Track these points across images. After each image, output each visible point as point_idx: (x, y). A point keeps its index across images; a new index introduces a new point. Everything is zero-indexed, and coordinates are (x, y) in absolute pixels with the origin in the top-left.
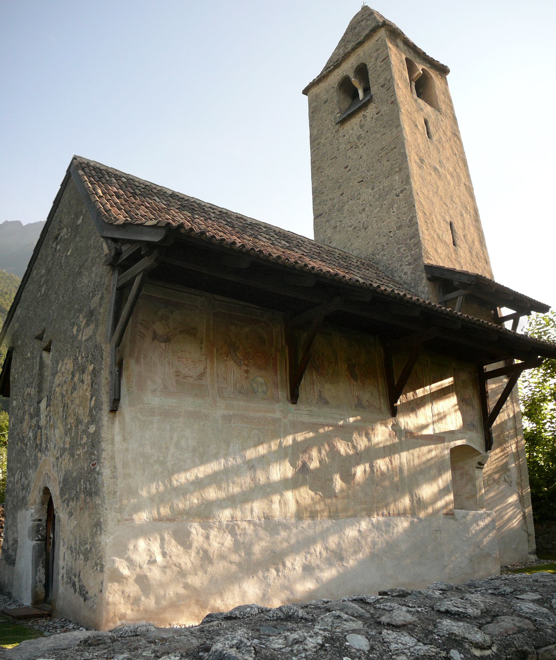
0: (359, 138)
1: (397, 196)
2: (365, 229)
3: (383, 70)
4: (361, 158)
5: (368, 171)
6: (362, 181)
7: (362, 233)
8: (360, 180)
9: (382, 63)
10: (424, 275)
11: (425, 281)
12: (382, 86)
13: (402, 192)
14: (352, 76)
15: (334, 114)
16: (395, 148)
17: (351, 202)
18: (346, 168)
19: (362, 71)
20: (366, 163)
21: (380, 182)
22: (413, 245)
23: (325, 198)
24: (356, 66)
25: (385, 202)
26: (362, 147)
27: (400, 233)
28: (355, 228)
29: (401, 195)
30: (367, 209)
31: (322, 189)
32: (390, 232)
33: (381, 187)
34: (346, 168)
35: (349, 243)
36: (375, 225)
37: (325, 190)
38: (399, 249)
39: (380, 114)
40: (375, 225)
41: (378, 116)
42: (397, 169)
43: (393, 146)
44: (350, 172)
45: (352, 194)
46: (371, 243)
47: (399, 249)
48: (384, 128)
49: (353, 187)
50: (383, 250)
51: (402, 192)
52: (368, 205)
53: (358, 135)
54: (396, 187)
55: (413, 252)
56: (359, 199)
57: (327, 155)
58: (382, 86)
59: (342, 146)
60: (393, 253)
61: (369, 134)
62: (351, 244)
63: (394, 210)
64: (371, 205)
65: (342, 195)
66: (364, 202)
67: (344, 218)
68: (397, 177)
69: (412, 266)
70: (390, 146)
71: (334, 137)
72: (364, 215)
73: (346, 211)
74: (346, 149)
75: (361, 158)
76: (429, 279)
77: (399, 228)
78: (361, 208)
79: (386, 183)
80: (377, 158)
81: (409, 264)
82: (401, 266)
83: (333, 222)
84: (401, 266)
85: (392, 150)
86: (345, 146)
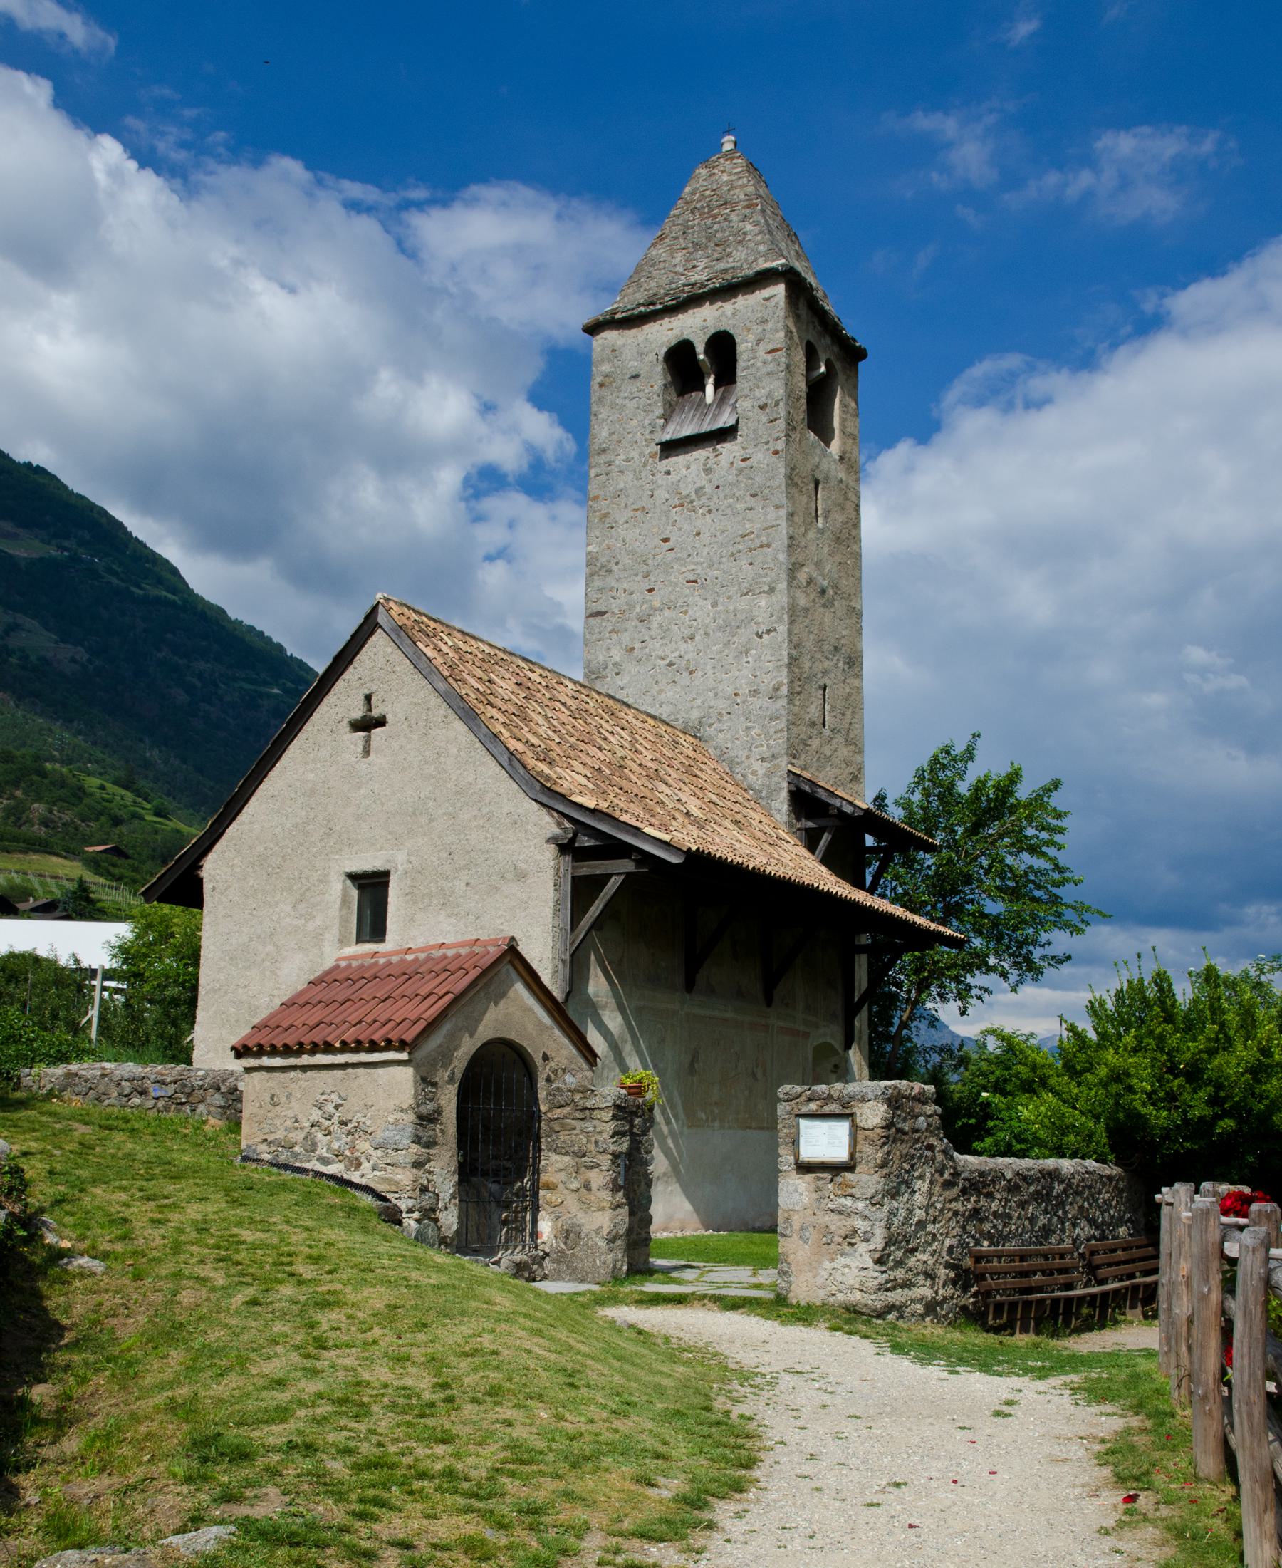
0: (699, 491)
1: (760, 636)
2: (691, 673)
3: (768, 374)
4: (698, 534)
5: (710, 566)
6: (695, 582)
7: (684, 679)
8: (692, 578)
9: (769, 357)
10: (785, 785)
11: (784, 795)
12: (762, 408)
13: (768, 631)
14: (700, 348)
15: (651, 416)
16: (768, 545)
17: (667, 613)
18: (666, 540)
19: (723, 345)
20: (706, 549)
21: (729, 598)
22: (773, 730)
23: (614, 584)
24: (712, 331)
25: (736, 639)
26: (703, 515)
27: (756, 703)
28: (671, 664)
29: (765, 636)
30: (697, 638)
31: (609, 562)
32: (736, 695)
33: (731, 608)
34: (666, 540)
35: (656, 688)
36: (710, 673)
37: (615, 568)
38: (748, 728)
39: (747, 463)
40: (710, 673)
41: (744, 464)
42: (766, 588)
43: (764, 540)
44: (671, 554)
45: (673, 597)
46: (699, 702)
47: (748, 728)
48: (753, 496)
49: (676, 585)
50: (720, 721)
51: (768, 631)
52: (701, 632)
53: (698, 485)
54: (760, 620)
55: (771, 742)
56: (686, 612)
57: (627, 496)
58: (762, 408)
59: (661, 494)
60: (737, 732)
61: (721, 492)
62: (660, 692)
63: (750, 659)
64: (707, 634)
65: (651, 590)
66: (695, 623)
67: (652, 638)
68: (763, 603)
69: (766, 765)
70: (758, 536)
71: (645, 465)
72: (690, 646)
73: (655, 626)
74: (670, 502)
75: (698, 534)
76: (790, 792)
77: (754, 693)
78: (687, 632)
79: (742, 604)
80: (731, 549)
81: (763, 760)
82: (748, 757)
83: (626, 637)
84: (748, 757)
85: (761, 546)
86: (667, 496)
